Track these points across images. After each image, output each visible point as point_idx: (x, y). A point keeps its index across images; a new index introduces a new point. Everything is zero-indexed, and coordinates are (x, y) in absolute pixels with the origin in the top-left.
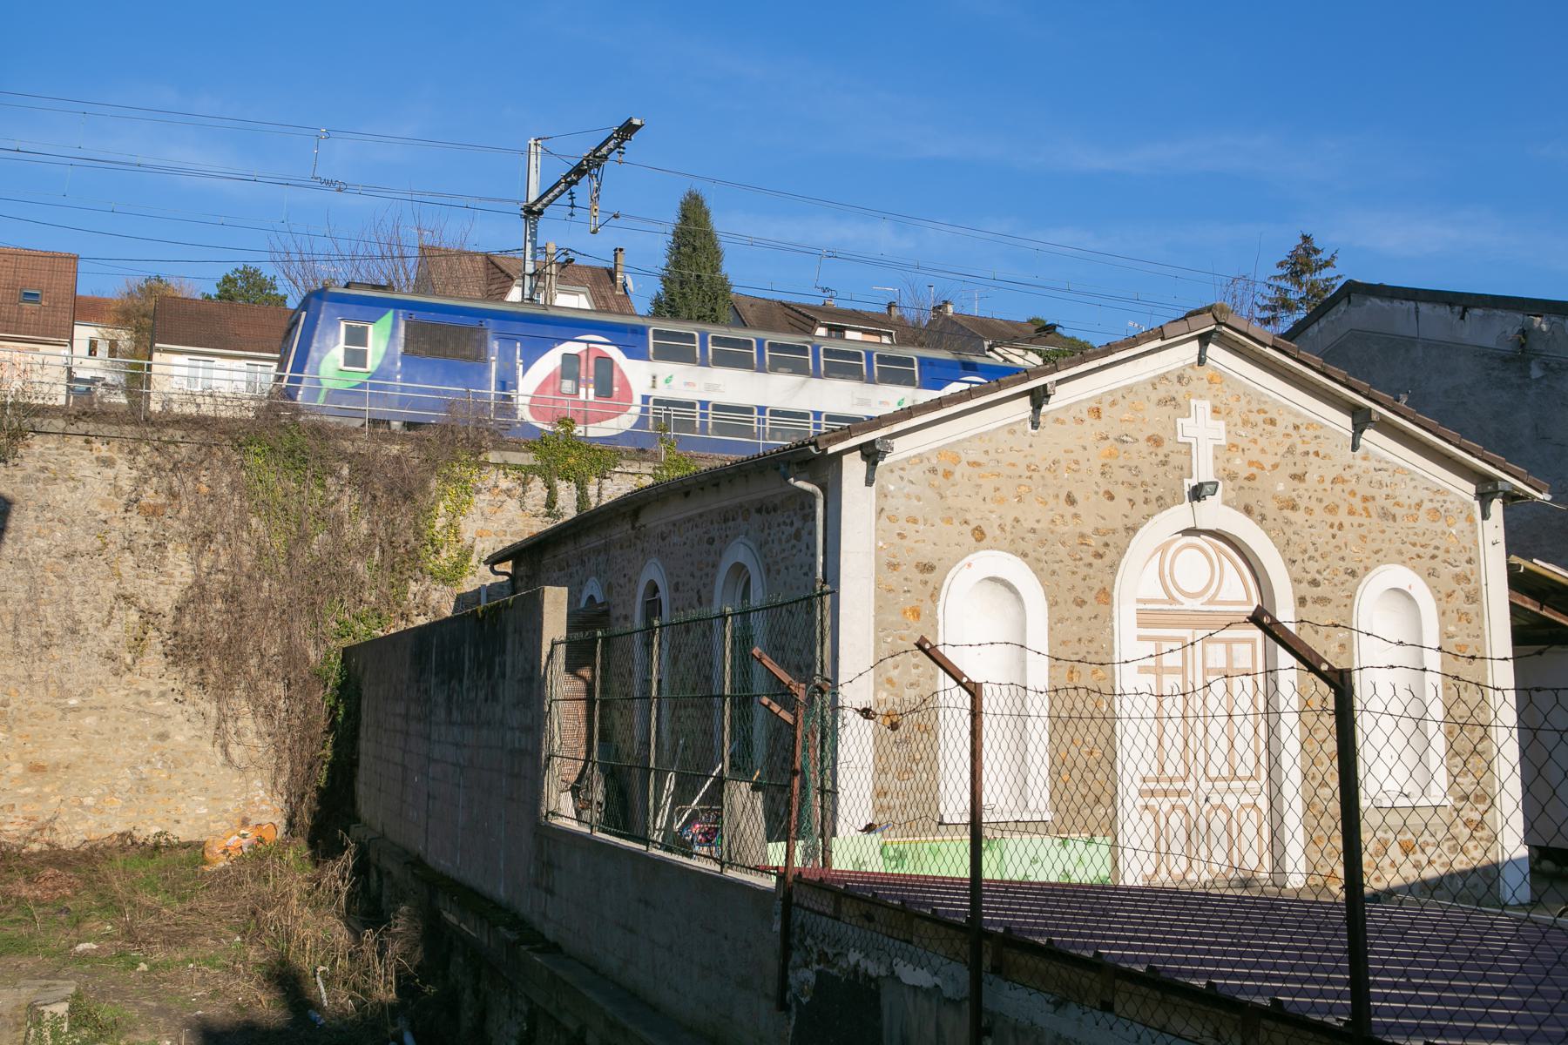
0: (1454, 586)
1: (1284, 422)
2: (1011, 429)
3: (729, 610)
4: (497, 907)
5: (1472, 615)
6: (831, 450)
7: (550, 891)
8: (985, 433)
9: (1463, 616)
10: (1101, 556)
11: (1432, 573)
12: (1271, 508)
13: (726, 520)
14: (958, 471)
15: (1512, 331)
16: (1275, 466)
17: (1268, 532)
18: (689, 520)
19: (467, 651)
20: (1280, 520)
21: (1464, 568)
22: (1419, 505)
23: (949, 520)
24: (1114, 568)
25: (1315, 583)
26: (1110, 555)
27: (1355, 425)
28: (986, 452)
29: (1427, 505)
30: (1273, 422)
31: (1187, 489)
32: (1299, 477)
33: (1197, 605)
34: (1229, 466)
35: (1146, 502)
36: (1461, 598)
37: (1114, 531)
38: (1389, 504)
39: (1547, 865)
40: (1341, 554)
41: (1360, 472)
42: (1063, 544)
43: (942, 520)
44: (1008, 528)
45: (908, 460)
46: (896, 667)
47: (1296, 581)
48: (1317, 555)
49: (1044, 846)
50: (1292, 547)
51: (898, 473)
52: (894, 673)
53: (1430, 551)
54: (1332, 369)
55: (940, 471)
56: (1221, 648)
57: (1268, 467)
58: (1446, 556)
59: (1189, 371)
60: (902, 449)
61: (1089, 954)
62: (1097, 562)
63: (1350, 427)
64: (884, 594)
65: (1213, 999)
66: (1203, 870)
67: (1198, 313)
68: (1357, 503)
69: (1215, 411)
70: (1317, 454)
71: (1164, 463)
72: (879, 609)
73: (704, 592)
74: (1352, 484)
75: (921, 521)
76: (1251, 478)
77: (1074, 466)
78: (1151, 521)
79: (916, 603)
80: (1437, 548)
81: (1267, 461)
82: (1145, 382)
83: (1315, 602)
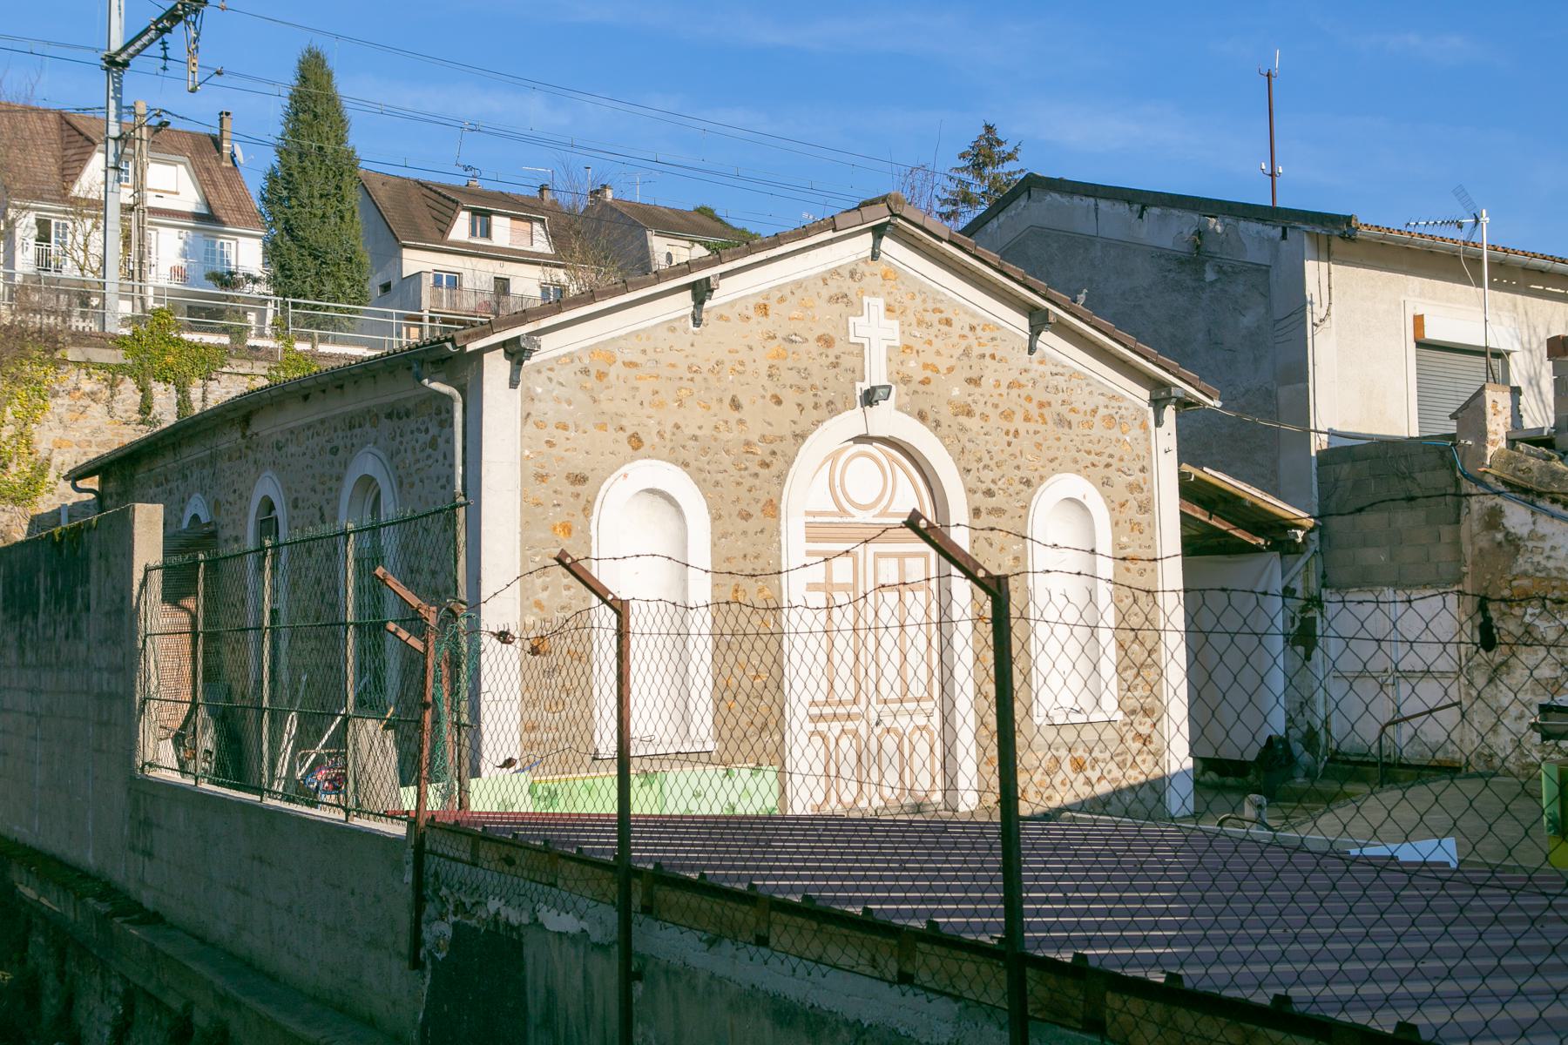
1: (961, 322)
3: (351, 526)
4: (85, 876)
5: (1144, 525)
6: (470, 347)
7: (148, 854)
8: (643, 330)
9: (1136, 527)
10: (768, 466)
11: (1106, 482)
12: (945, 414)
13: (351, 427)
14: (613, 372)
15: (1188, 232)
16: (951, 369)
17: (942, 439)
19: (42, 582)
20: (955, 427)
22: (1094, 412)
23: (602, 427)
24: (781, 478)
25: (989, 493)
26: (778, 464)
29: (1102, 412)
30: (948, 322)
31: (859, 393)
32: (974, 381)
35: (816, 407)
36: (1133, 507)
37: (782, 439)
38: (1064, 410)
39: (1211, 776)
40: (1016, 463)
41: (1036, 376)
42: (727, 452)
43: (596, 426)
45: (557, 359)
46: (545, 589)
47: (971, 491)
48: (992, 464)
51: (546, 374)
52: (543, 596)
53: (1105, 459)
54: (1010, 267)
55: (593, 372)
56: (894, 562)
57: (943, 370)
60: (551, 347)
61: (742, 887)
62: (764, 472)
64: (531, 508)
65: (868, 925)
66: (875, 797)
67: (873, 202)
68: (1033, 409)
69: (889, 309)
70: (993, 357)
71: (835, 365)
72: (525, 525)
73: (327, 510)
74: (1028, 390)
75: (572, 427)
77: (739, 368)
79: (566, 518)
80: (1111, 456)
81: (943, 364)
82: (816, 277)
83: (990, 513)
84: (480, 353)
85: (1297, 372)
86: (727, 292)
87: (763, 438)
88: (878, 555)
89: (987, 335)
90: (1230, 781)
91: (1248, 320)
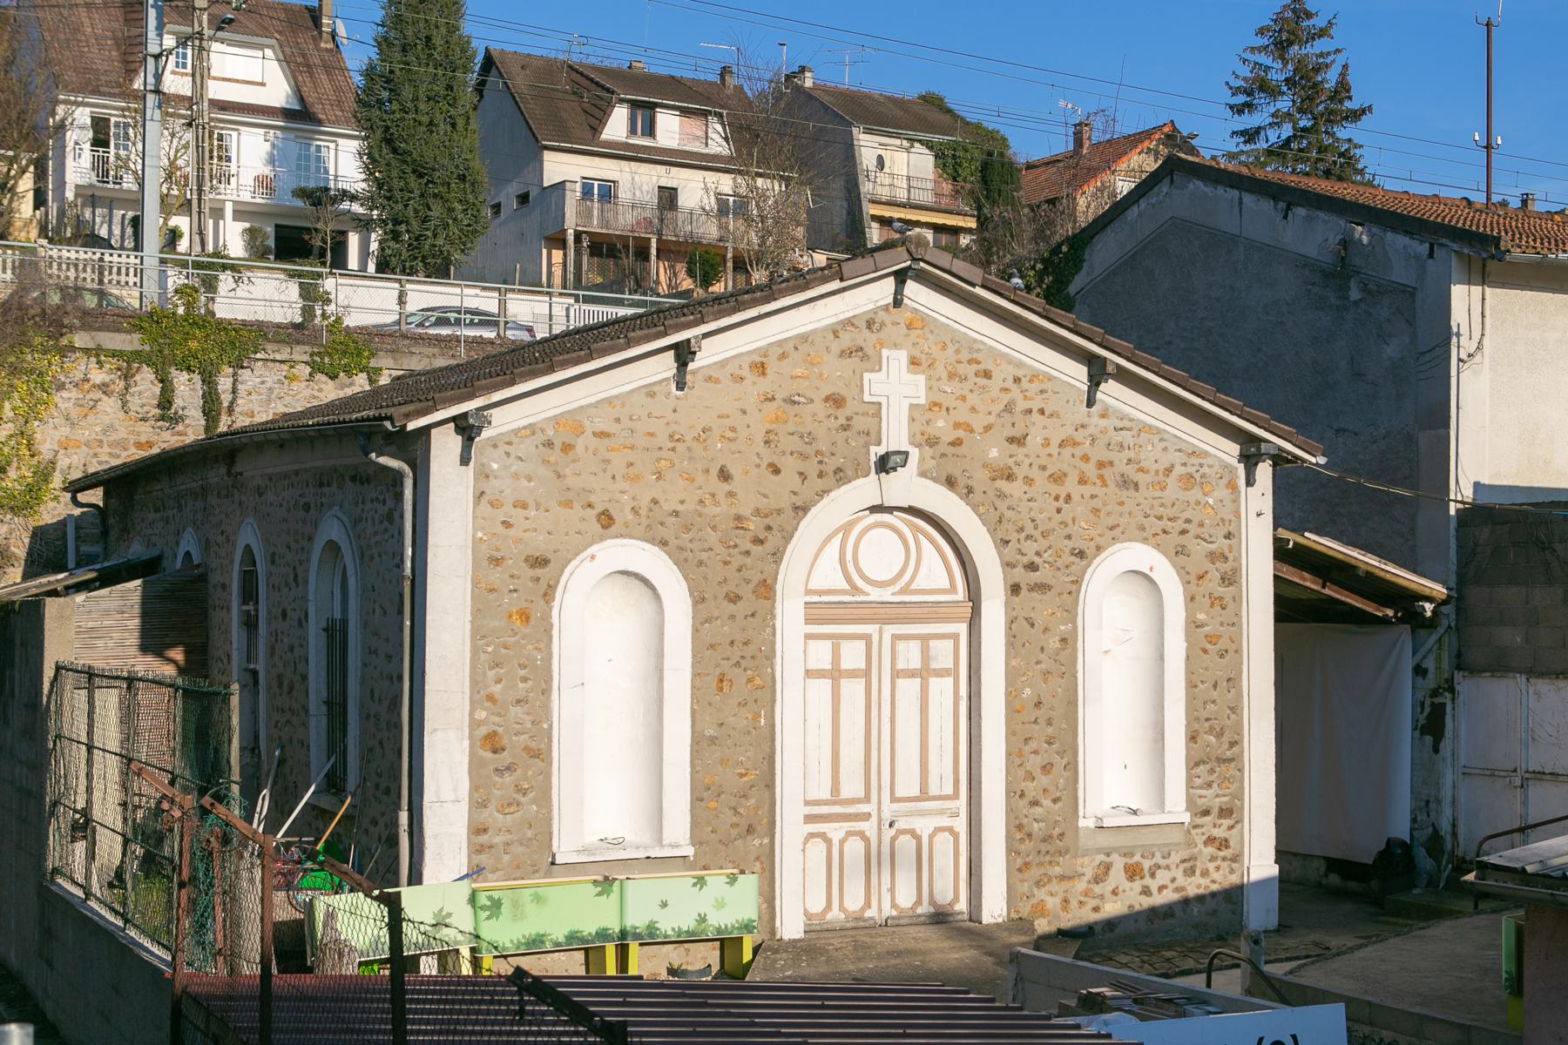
0: (1208, 566)
1: (1002, 374)
2: (650, 391)
5: (1228, 599)
6: (411, 426)
7: (49, 963)
8: (617, 397)
9: (1217, 602)
10: (761, 542)
11: (1181, 551)
12: (980, 478)
13: (321, 485)
14: (580, 443)
15: (1334, 240)
16: (988, 428)
17: (975, 508)
18: (285, 476)
20: (991, 494)
21: (1221, 544)
22: (1169, 471)
23: (568, 504)
24: (777, 556)
25: (1032, 567)
26: (773, 540)
27: (1091, 377)
28: (618, 420)
29: (1179, 470)
30: (987, 375)
31: (873, 459)
33: (886, 595)
34: (930, 430)
35: (821, 475)
36: (1213, 582)
37: (779, 512)
38: (1130, 471)
39: (1334, 879)
40: (1067, 531)
41: (1096, 432)
42: (714, 528)
43: (560, 504)
44: (643, 512)
45: (516, 432)
46: (499, 681)
47: (1008, 565)
48: (1037, 534)
49: (678, 886)
50: (1005, 525)
51: (503, 448)
52: (496, 689)
53: (1180, 525)
54: (1057, 312)
55: (558, 444)
56: (915, 646)
57: (978, 428)
58: (1199, 531)
59: (882, 313)
60: (504, 421)
63: (1085, 378)
64: (483, 595)
68: (1091, 470)
69: (914, 362)
70: (1042, 412)
71: (845, 428)
72: (477, 613)
73: (300, 570)
74: (1086, 447)
75: (532, 505)
76: (957, 443)
77: (730, 435)
78: (826, 499)
79: (524, 605)
80: (1188, 521)
81: (978, 422)
82: (824, 329)
83: (1031, 589)
84: (426, 430)
85: (1436, 416)
86: (709, 354)
87: (757, 512)
88: (896, 638)
89: (1035, 386)
90: (1352, 885)
91: (1391, 350)
